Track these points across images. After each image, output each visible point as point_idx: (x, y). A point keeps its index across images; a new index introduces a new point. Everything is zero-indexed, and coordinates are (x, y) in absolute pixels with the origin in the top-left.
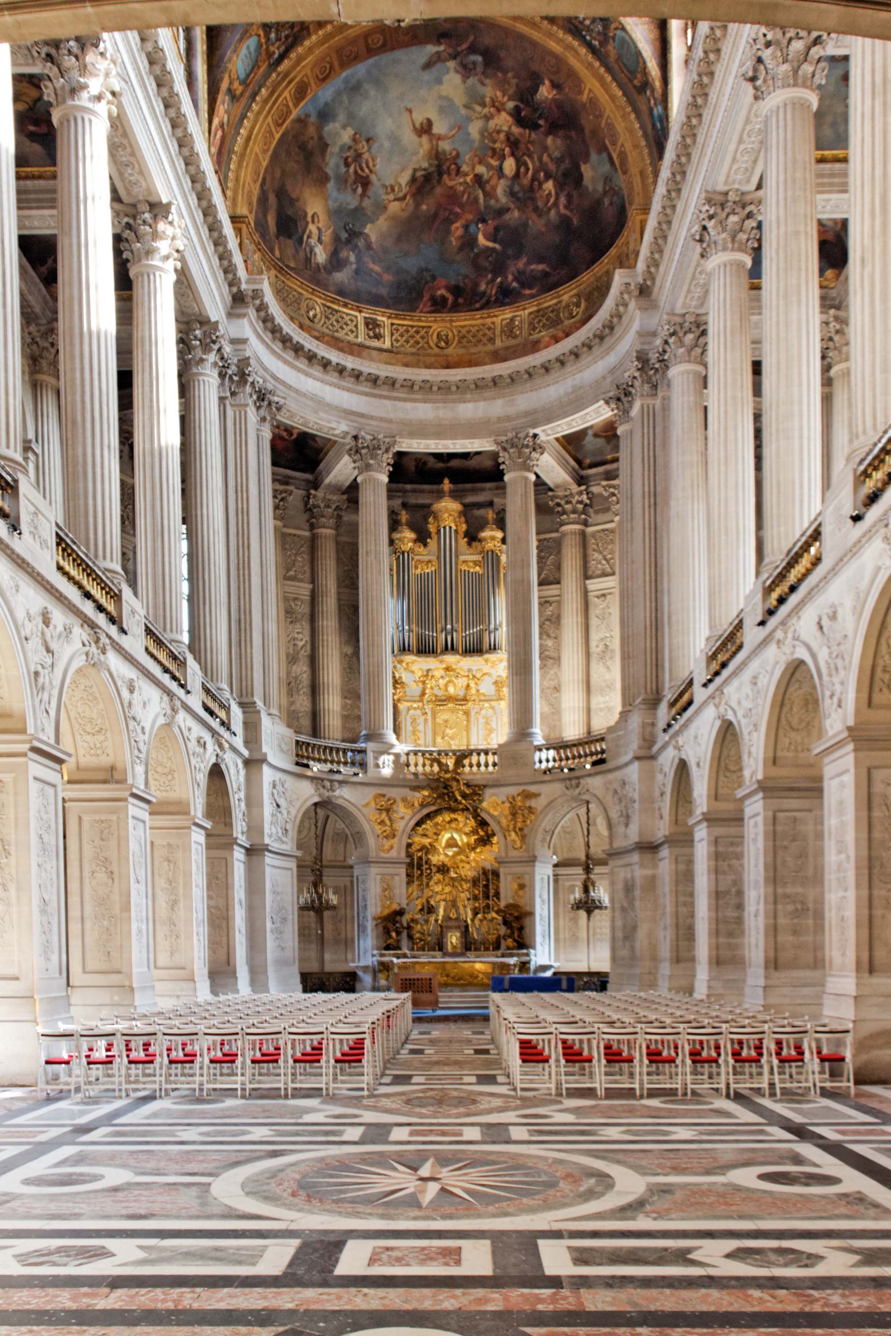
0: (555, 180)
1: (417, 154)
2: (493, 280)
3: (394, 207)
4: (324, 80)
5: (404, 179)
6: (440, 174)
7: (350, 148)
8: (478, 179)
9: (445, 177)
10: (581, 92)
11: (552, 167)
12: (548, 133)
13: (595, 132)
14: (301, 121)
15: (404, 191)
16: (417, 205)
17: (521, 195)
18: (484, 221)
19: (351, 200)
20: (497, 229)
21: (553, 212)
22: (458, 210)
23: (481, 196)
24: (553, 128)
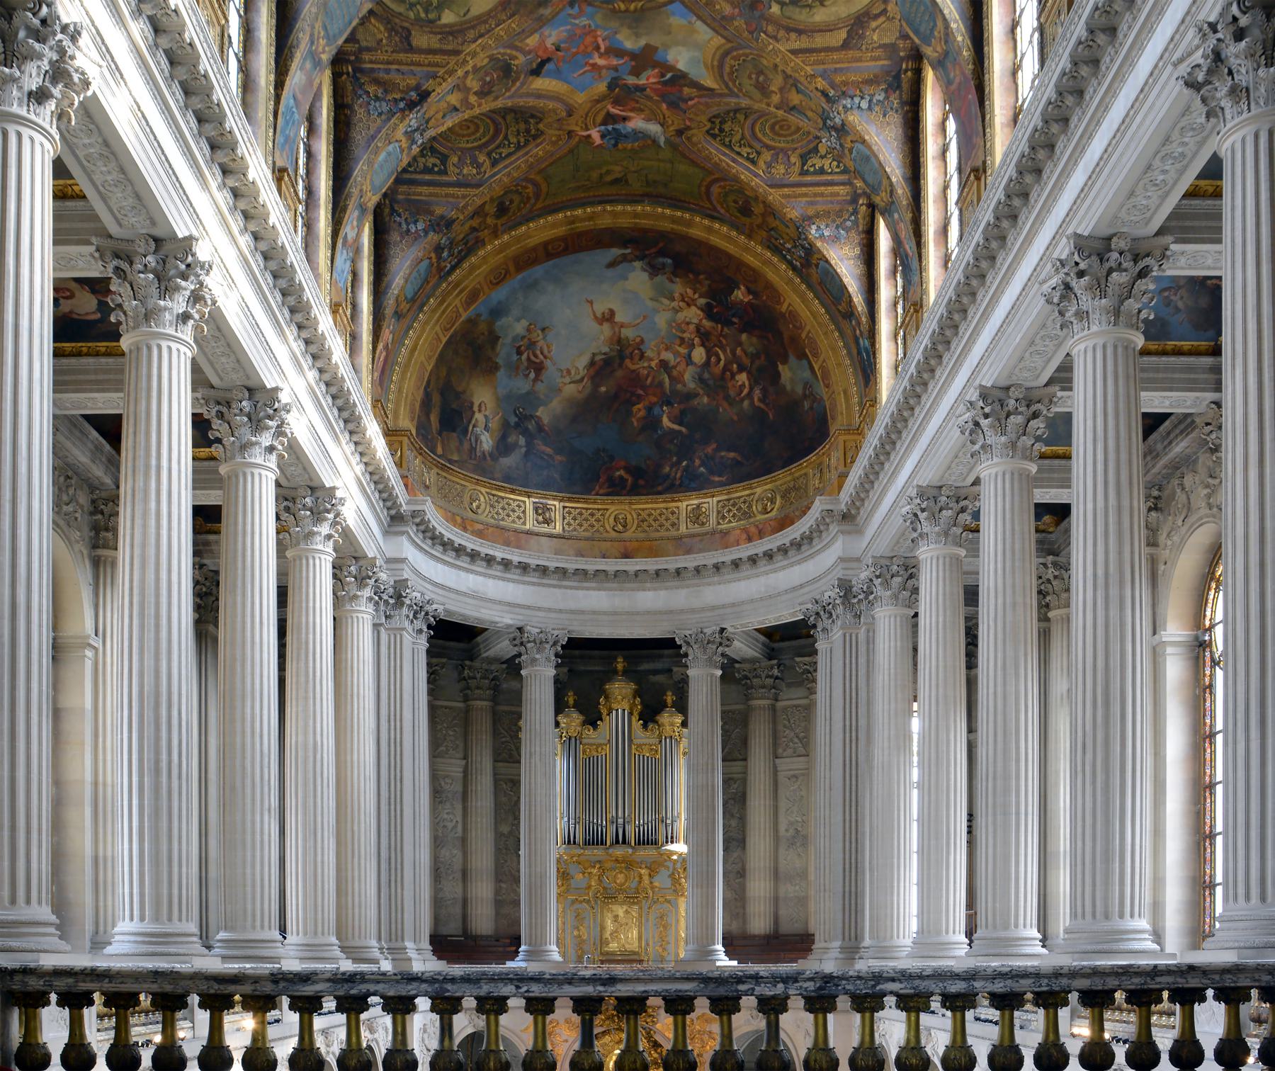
0: (749, 373)
1: (598, 340)
2: (679, 462)
3: (570, 390)
4: (497, 284)
5: (583, 361)
6: (621, 356)
7: (523, 337)
8: (664, 364)
9: (628, 362)
10: (779, 303)
11: (747, 361)
12: (742, 331)
13: (795, 340)
14: (472, 322)
15: (582, 372)
16: (596, 386)
17: (711, 382)
18: (669, 403)
19: (522, 385)
20: (683, 412)
21: (746, 403)
22: (641, 392)
23: (667, 380)
24: (747, 327)
